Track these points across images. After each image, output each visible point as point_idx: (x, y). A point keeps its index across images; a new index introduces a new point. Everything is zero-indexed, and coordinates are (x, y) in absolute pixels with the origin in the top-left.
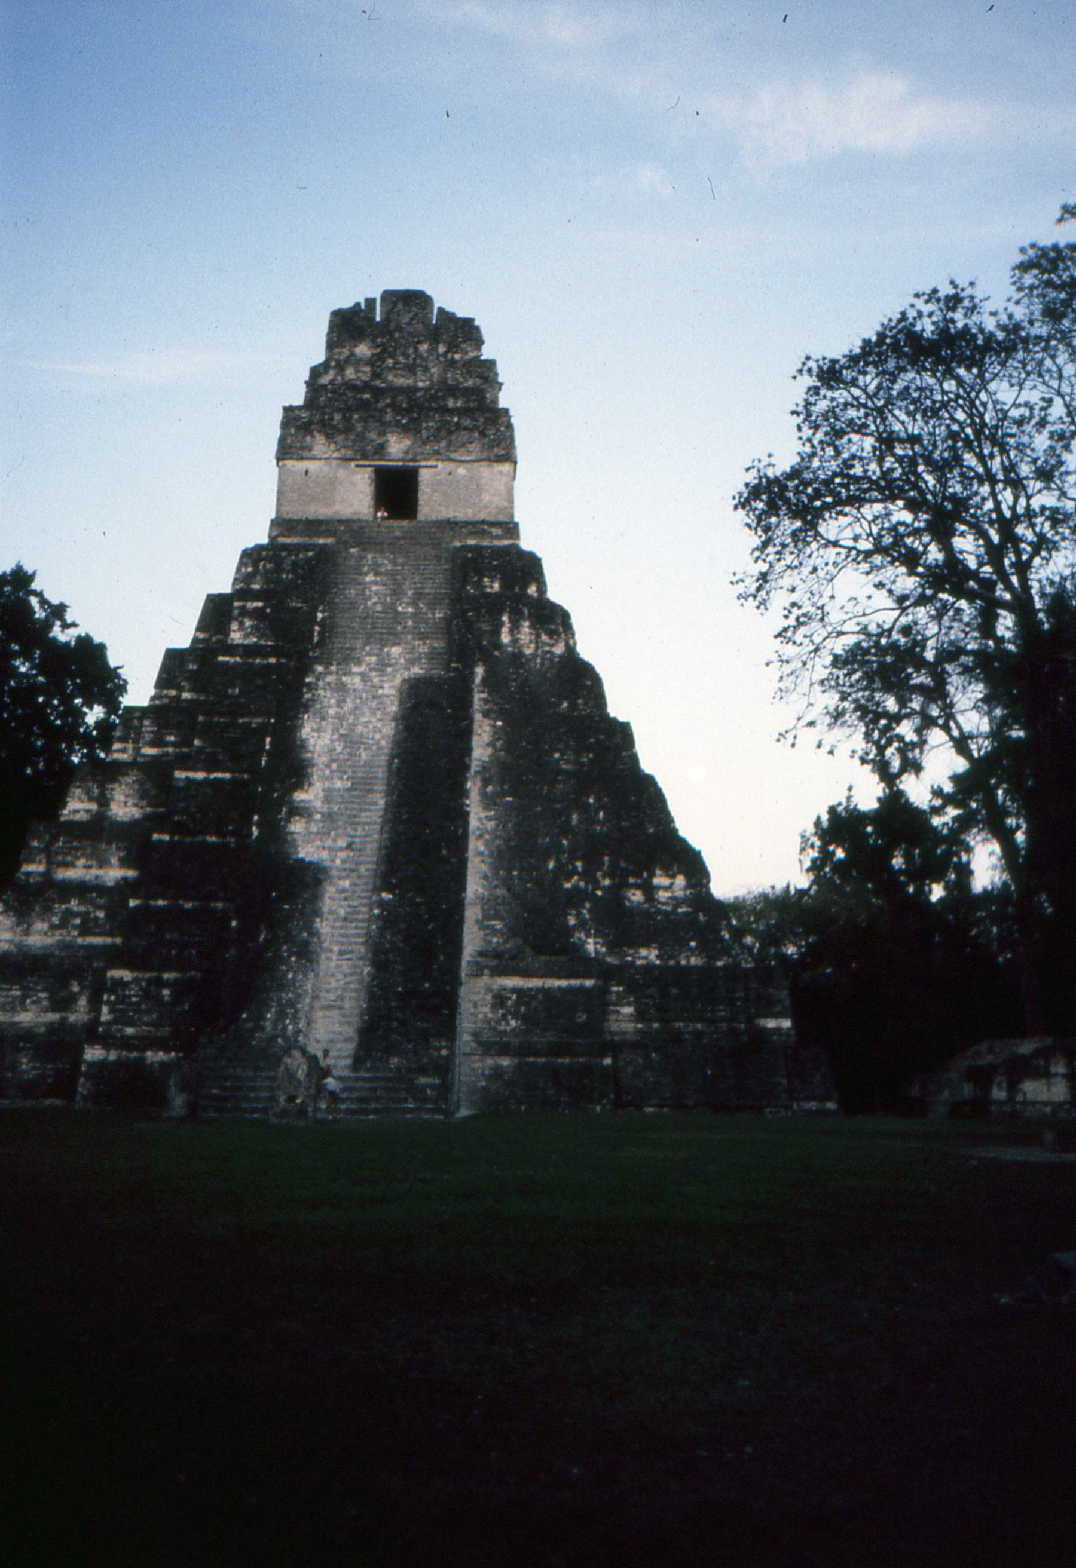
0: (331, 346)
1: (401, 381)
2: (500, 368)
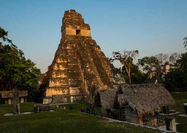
2: (84, 20)
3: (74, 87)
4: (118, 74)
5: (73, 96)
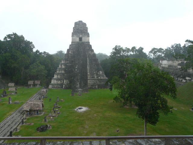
0: (75, 26)
1: (81, 29)
3: (67, 79)
4: (100, 72)
5: (65, 85)
